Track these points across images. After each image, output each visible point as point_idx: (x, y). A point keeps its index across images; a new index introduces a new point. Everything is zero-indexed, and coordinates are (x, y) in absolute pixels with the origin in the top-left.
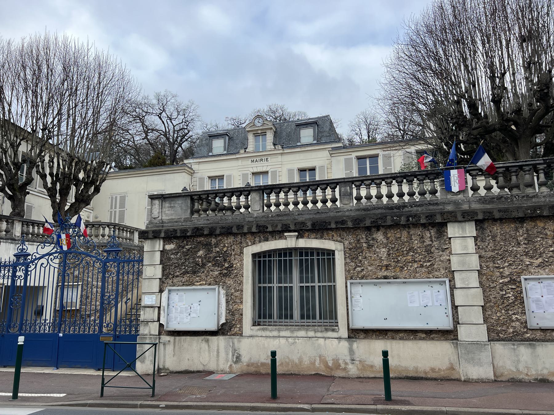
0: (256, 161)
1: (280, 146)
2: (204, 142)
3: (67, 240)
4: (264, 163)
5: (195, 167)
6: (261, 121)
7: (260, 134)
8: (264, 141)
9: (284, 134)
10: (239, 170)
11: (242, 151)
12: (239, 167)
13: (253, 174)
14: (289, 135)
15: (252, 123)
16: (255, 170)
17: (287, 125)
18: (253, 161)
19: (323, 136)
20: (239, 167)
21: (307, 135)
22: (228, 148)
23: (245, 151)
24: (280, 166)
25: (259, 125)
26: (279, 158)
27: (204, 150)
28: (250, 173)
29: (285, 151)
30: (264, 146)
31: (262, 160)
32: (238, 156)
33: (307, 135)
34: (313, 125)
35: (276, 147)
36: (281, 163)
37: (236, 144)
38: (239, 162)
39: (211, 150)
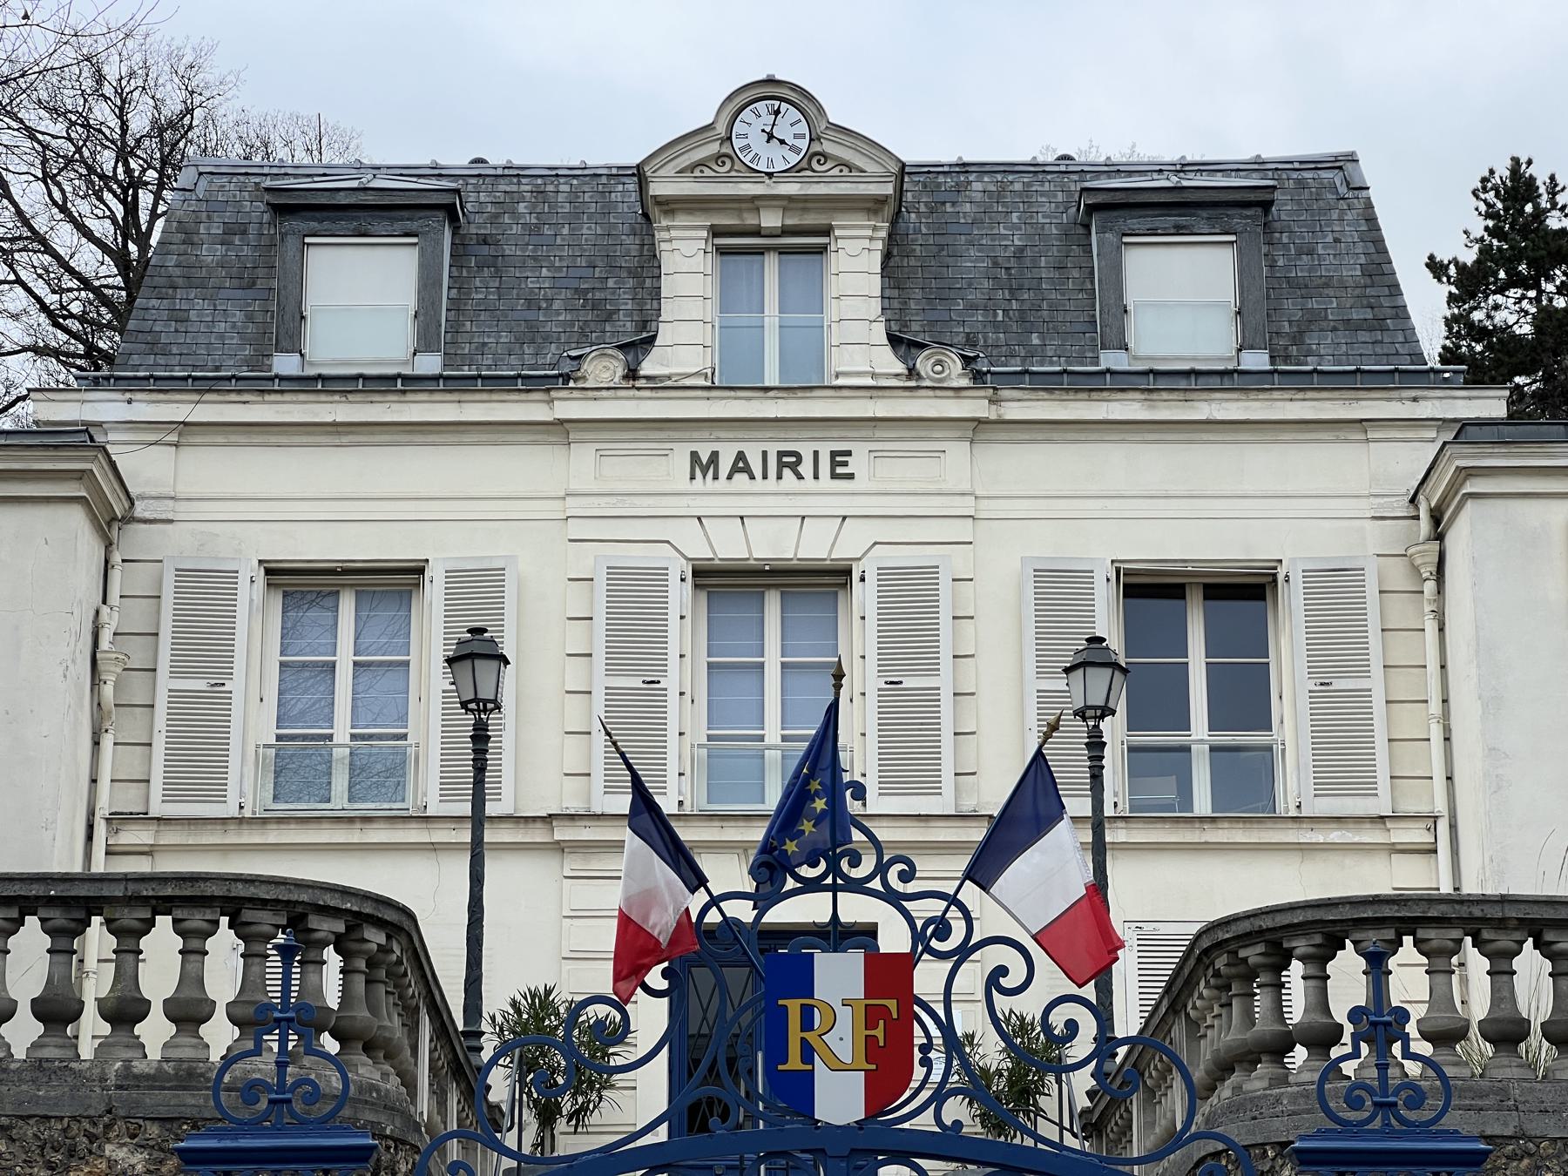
0: (741, 465)
1: (956, 366)
2: (210, 253)
3: (872, 1016)
4: (816, 492)
5: (144, 467)
6: (791, 125)
7: (770, 237)
8: (808, 297)
9: (972, 263)
10: (577, 529)
11: (603, 369)
12: (574, 506)
13: (706, 576)
14: (1012, 275)
15: (713, 146)
16: (729, 546)
17: (999, 195)
18: (704, 466)
19: (1313, 319)
20: (574, 506)
21: (1180, 297)
22: (455, 328)
23: (632, 374)
24: (962, 530)
25: (781, 159)
26: (956, 462)
27: (219, 325)
28: (678, 568)
29: (1013, 411)
30: (806, 346)
31: (789, 462)
32: (569, 408)
33: (1180, 297)
34: (1238, 219)
35: (924, 363)
36: (966, 506)
37: (531, 303)
38: (581, 465)
39: (286, 325)
